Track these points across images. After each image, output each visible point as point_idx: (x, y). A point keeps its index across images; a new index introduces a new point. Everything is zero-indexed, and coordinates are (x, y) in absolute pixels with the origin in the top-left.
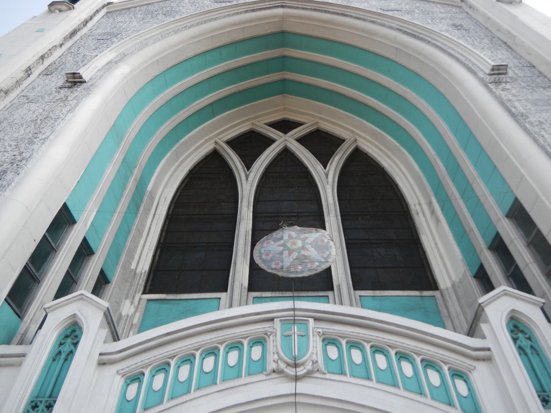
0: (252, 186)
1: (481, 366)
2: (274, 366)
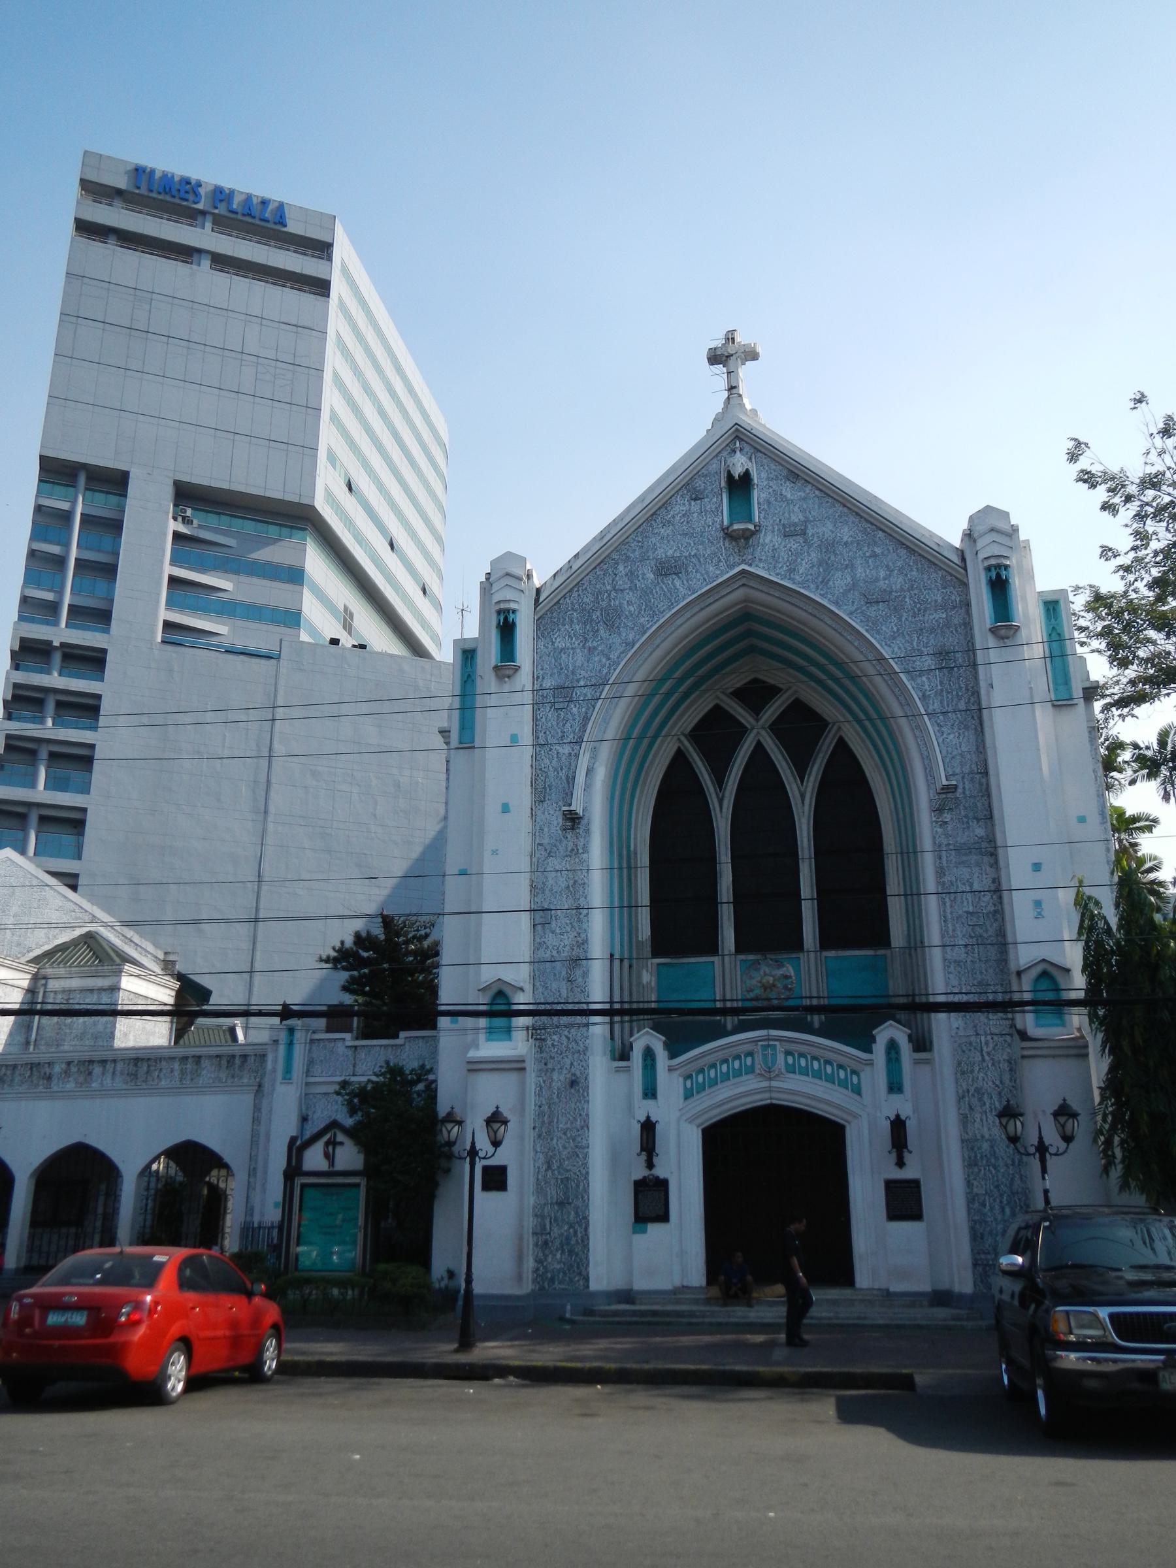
0: (727, 819)
1: (868, 1069)
2: (758, 1071)
